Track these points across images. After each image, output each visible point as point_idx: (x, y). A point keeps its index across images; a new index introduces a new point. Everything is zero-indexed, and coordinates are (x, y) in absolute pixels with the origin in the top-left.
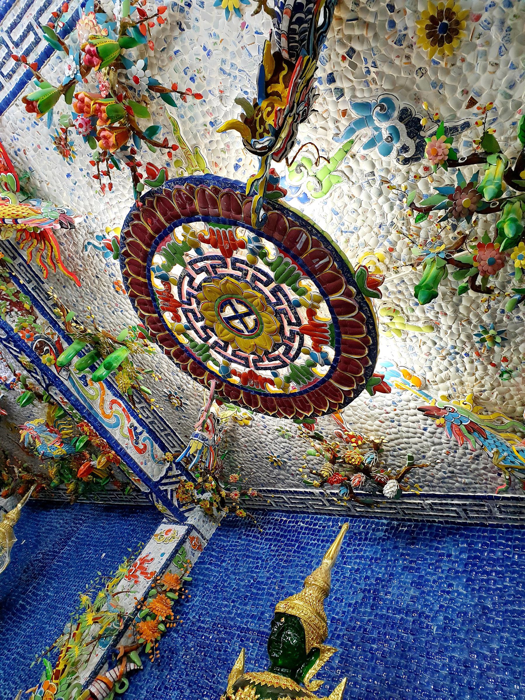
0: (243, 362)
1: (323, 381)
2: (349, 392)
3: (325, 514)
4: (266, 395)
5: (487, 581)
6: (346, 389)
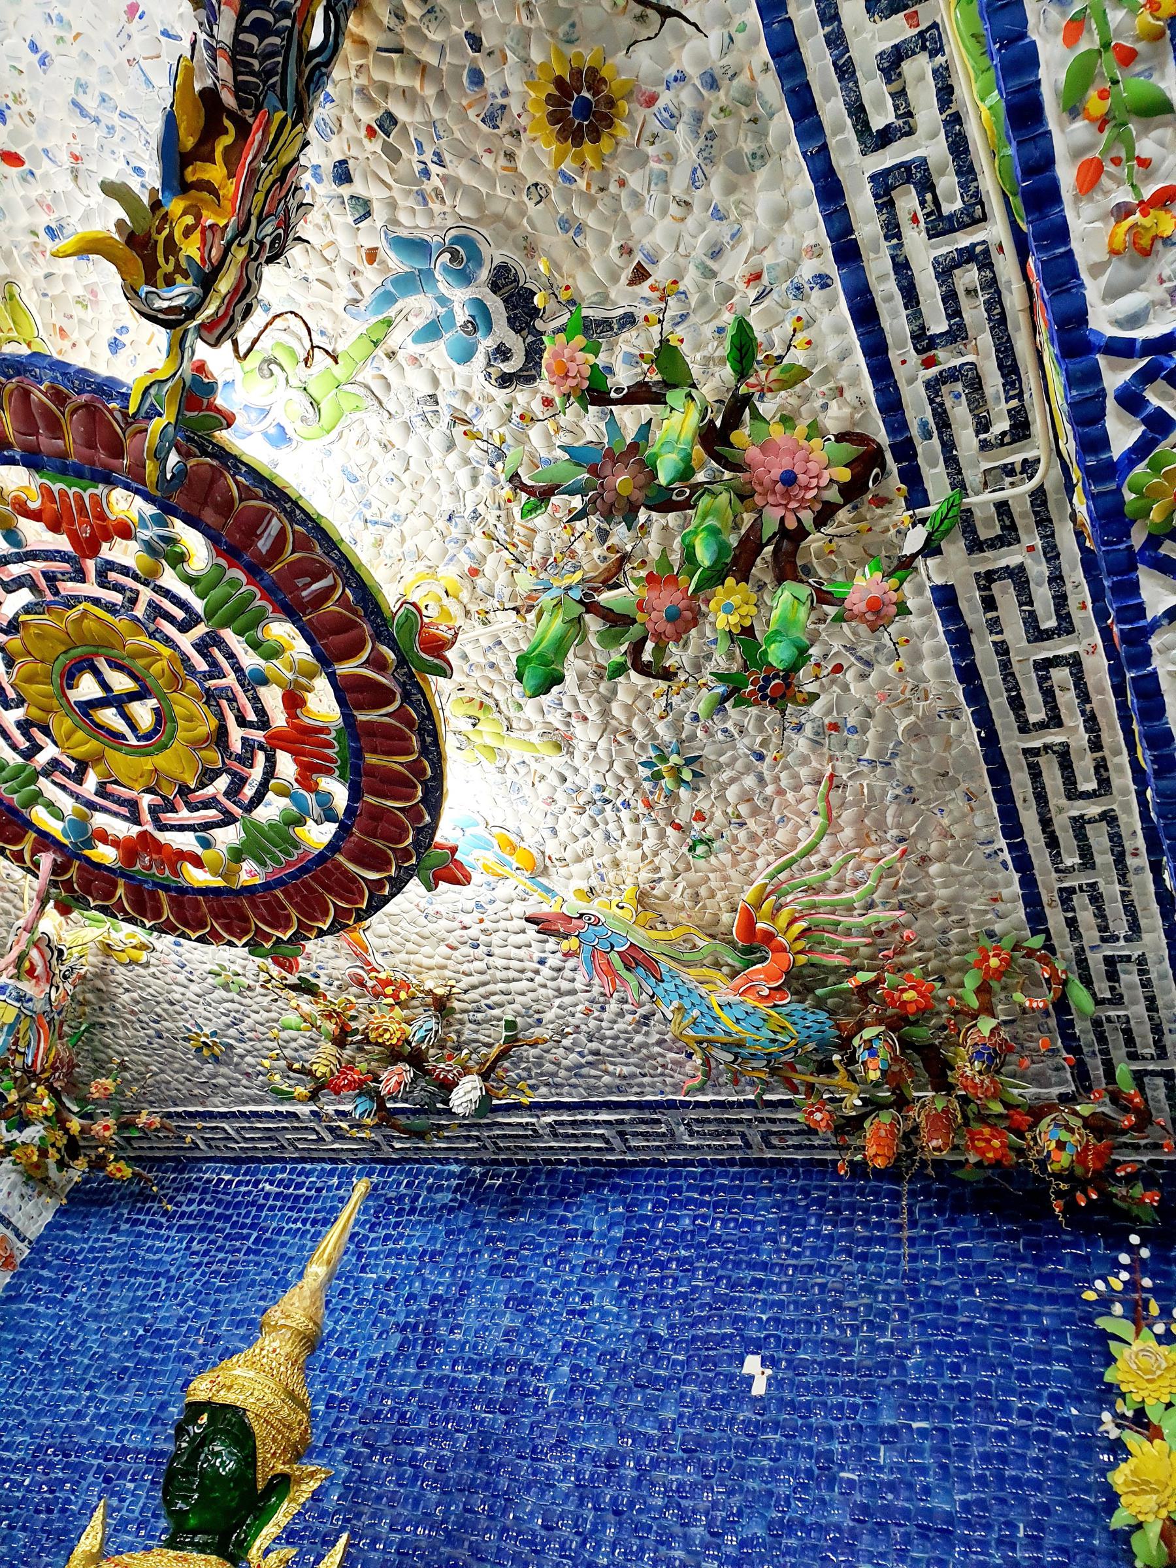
0: (124, 811)
1: (322, 857)
2: (379, 884)
3: (322, 1160)
4: (183, 891)
5: (660, 1281)
6: (373, 876)
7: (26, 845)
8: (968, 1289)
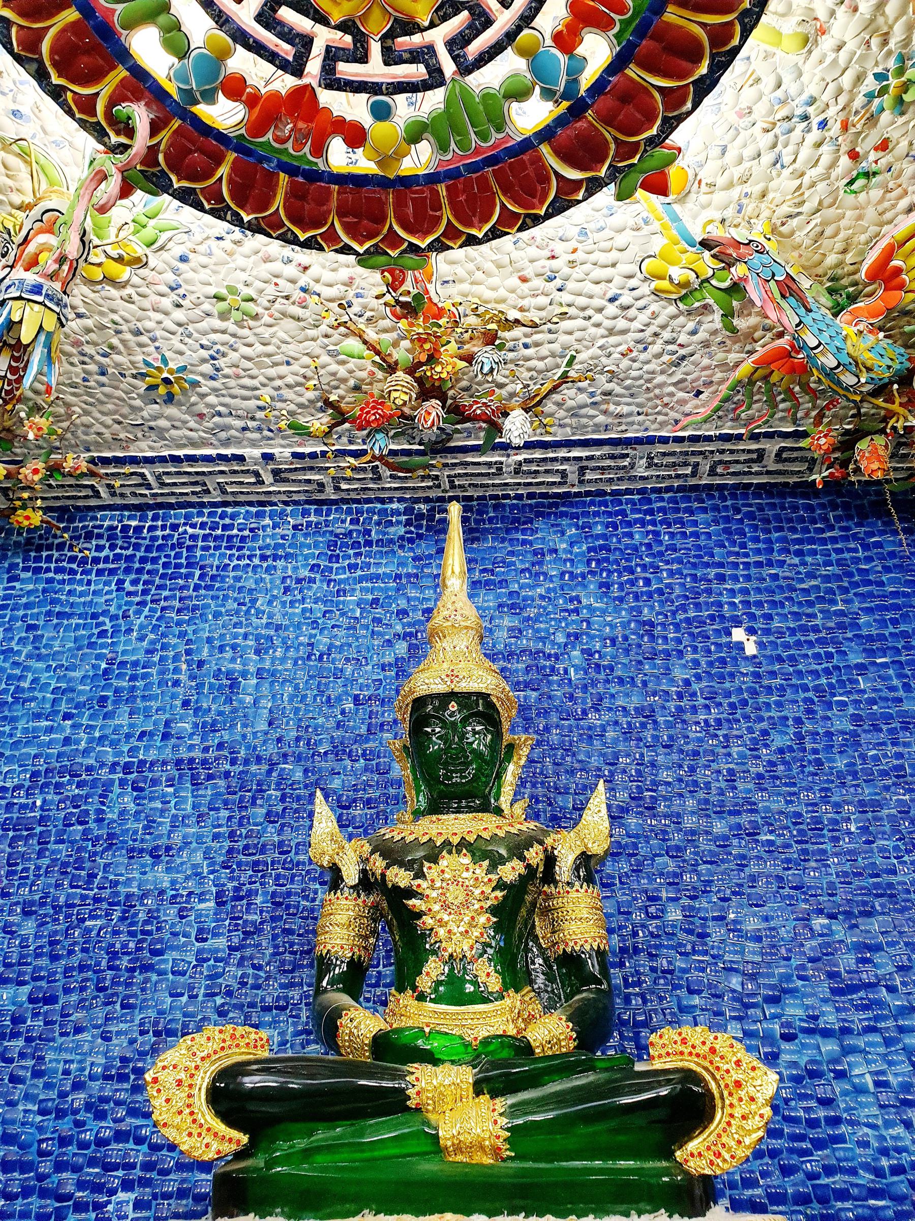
0: (287, 50)
1: (527, 145)
2: (577, 184)
3: (250, 504)
4: (314, 176)
6: (574, 174)
7: (105, 89)
8: (887, 569)
